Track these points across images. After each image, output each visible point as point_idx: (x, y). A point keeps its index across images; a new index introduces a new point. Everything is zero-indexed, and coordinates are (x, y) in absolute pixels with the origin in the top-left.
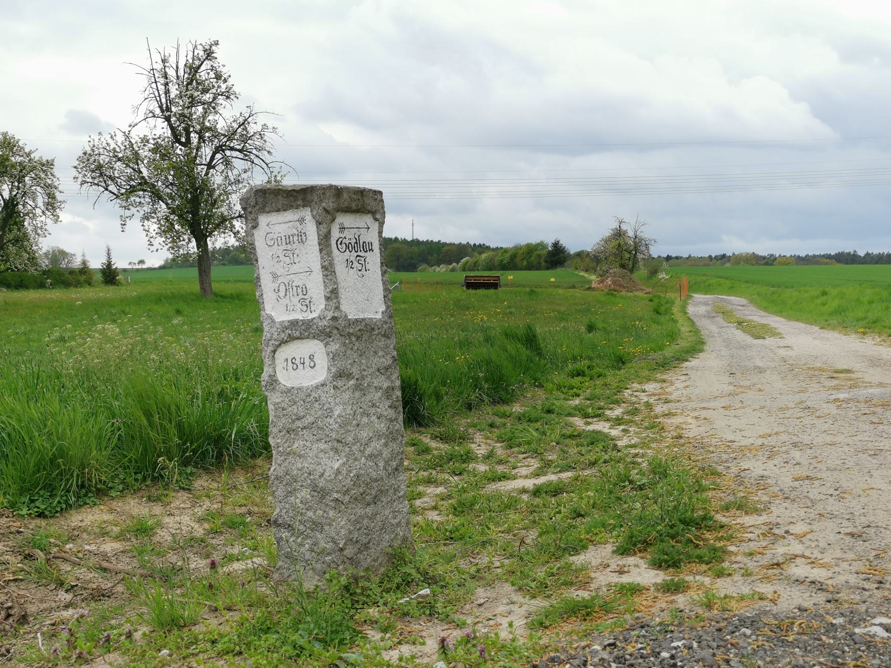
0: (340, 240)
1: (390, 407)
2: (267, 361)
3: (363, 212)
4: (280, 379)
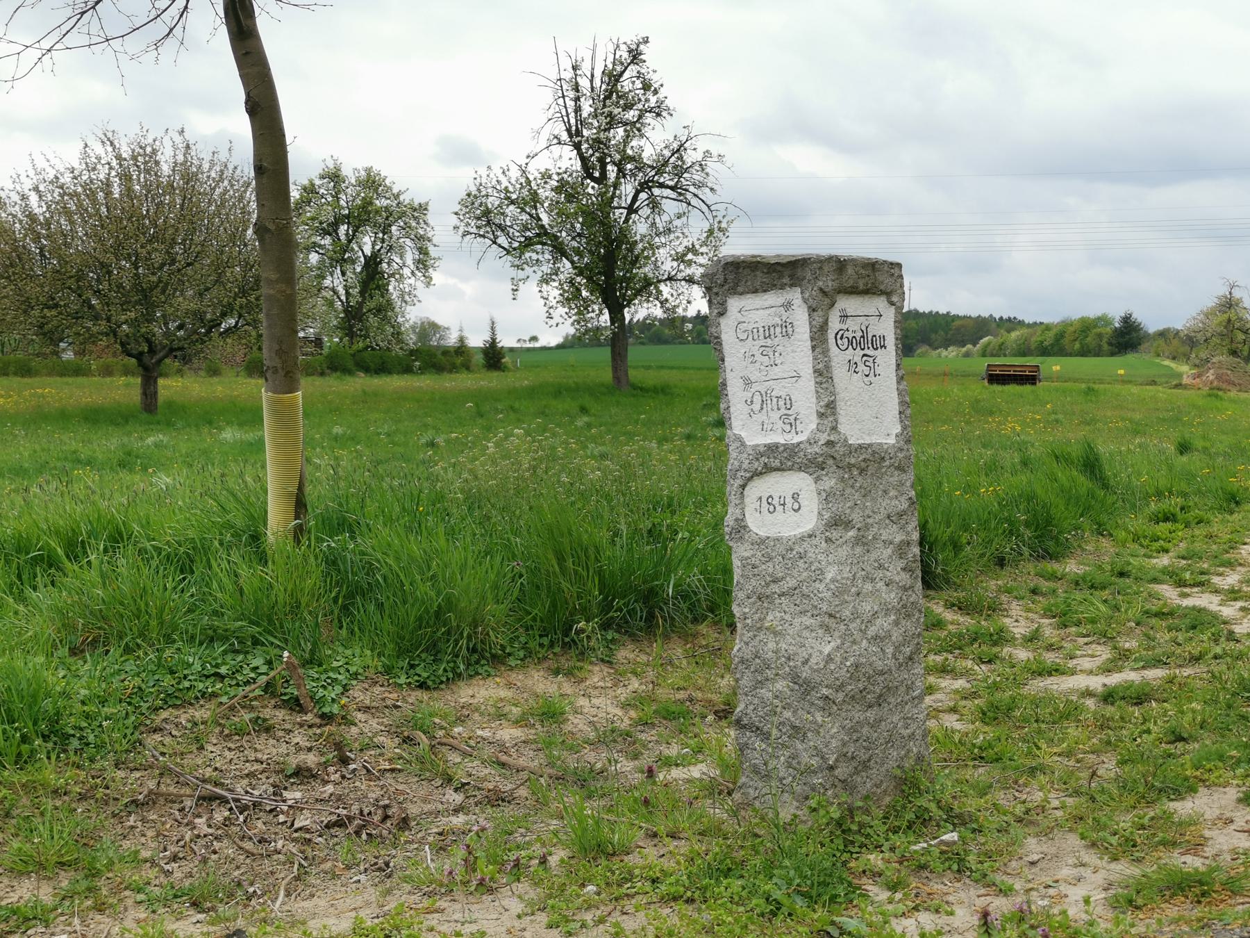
0: (841, 333)
1: (904, 569)
2: (733, 499)
3: (874, 294)
4: (750, 525)
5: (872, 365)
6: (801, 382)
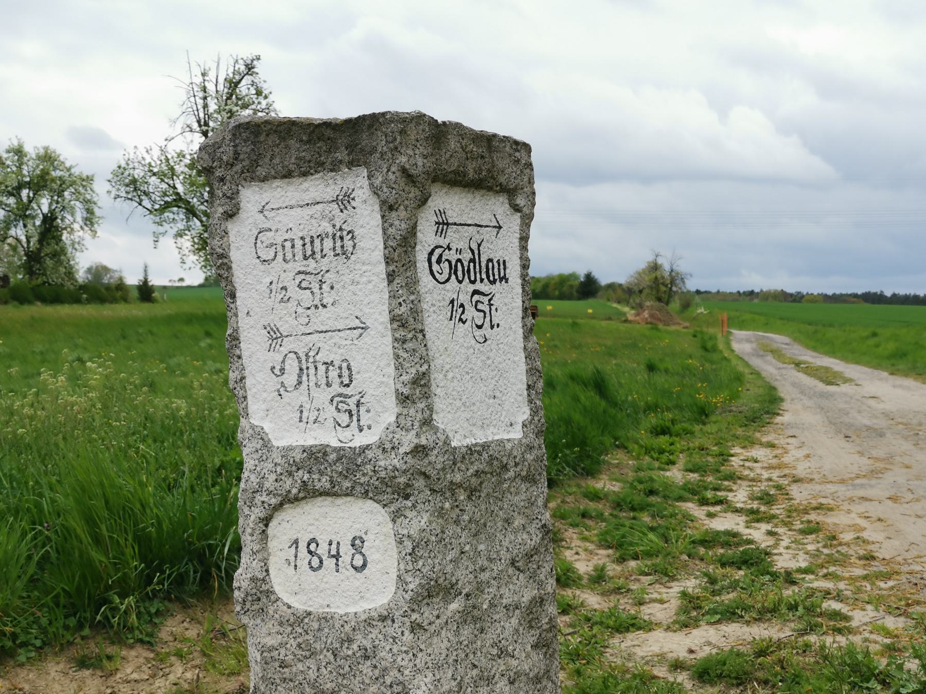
0: (438, 252)
1: (535, 647)
2: (249, 543)
3: (490, 189)
4: (277, 588)
5: (487, 309)
6: (367, 338)
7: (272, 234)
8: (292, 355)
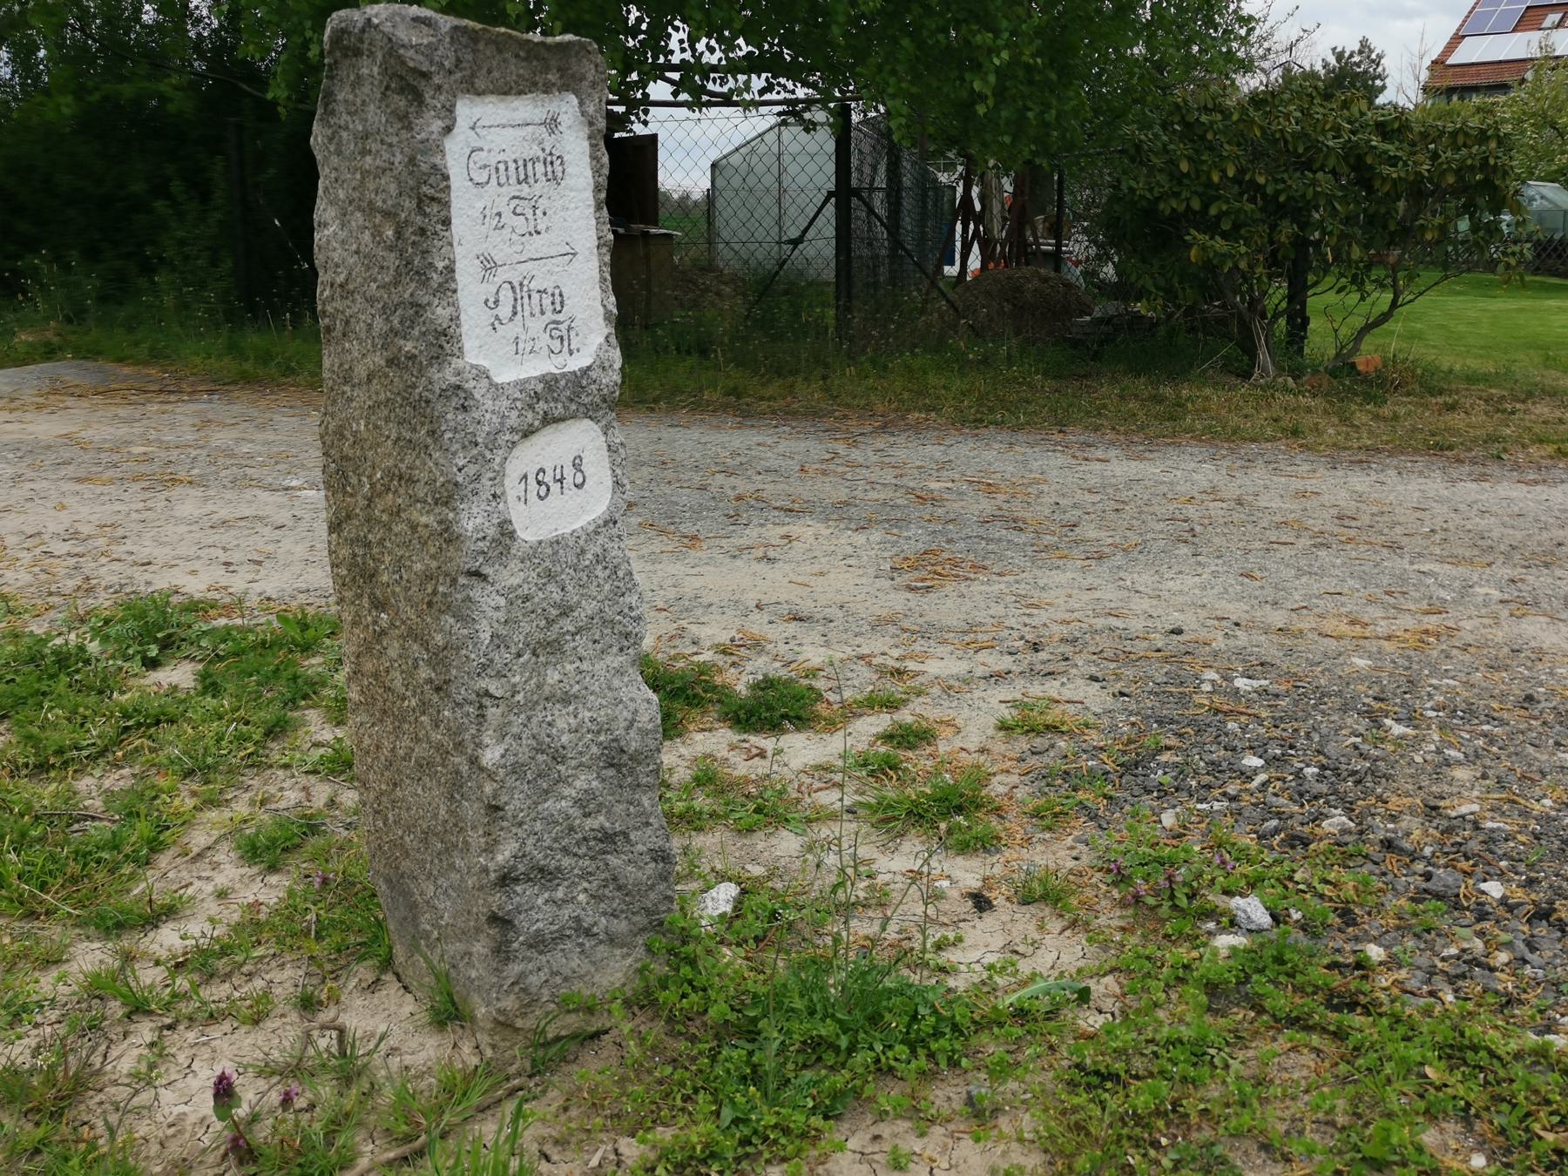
6: (578, 263)
7: (484, 154)
8: (507, 286)
